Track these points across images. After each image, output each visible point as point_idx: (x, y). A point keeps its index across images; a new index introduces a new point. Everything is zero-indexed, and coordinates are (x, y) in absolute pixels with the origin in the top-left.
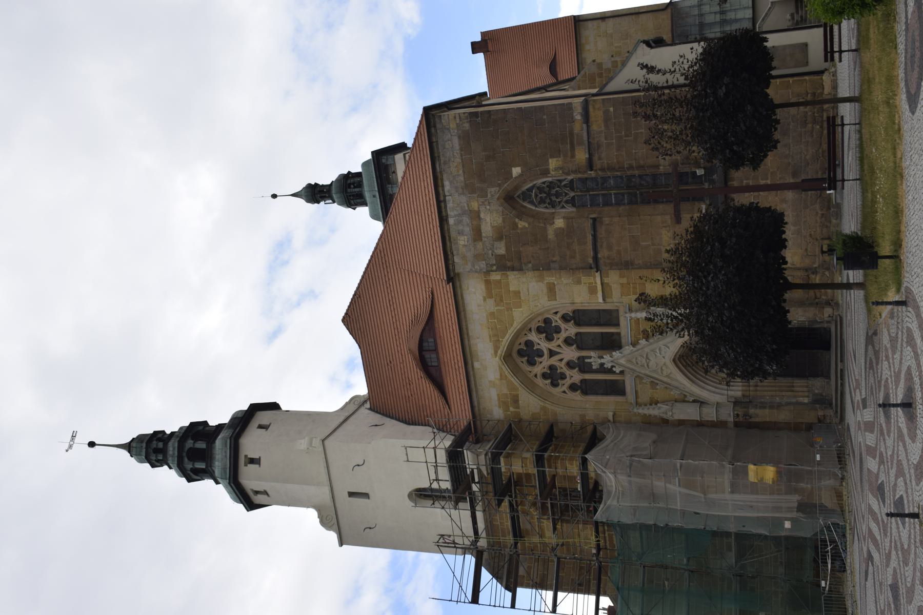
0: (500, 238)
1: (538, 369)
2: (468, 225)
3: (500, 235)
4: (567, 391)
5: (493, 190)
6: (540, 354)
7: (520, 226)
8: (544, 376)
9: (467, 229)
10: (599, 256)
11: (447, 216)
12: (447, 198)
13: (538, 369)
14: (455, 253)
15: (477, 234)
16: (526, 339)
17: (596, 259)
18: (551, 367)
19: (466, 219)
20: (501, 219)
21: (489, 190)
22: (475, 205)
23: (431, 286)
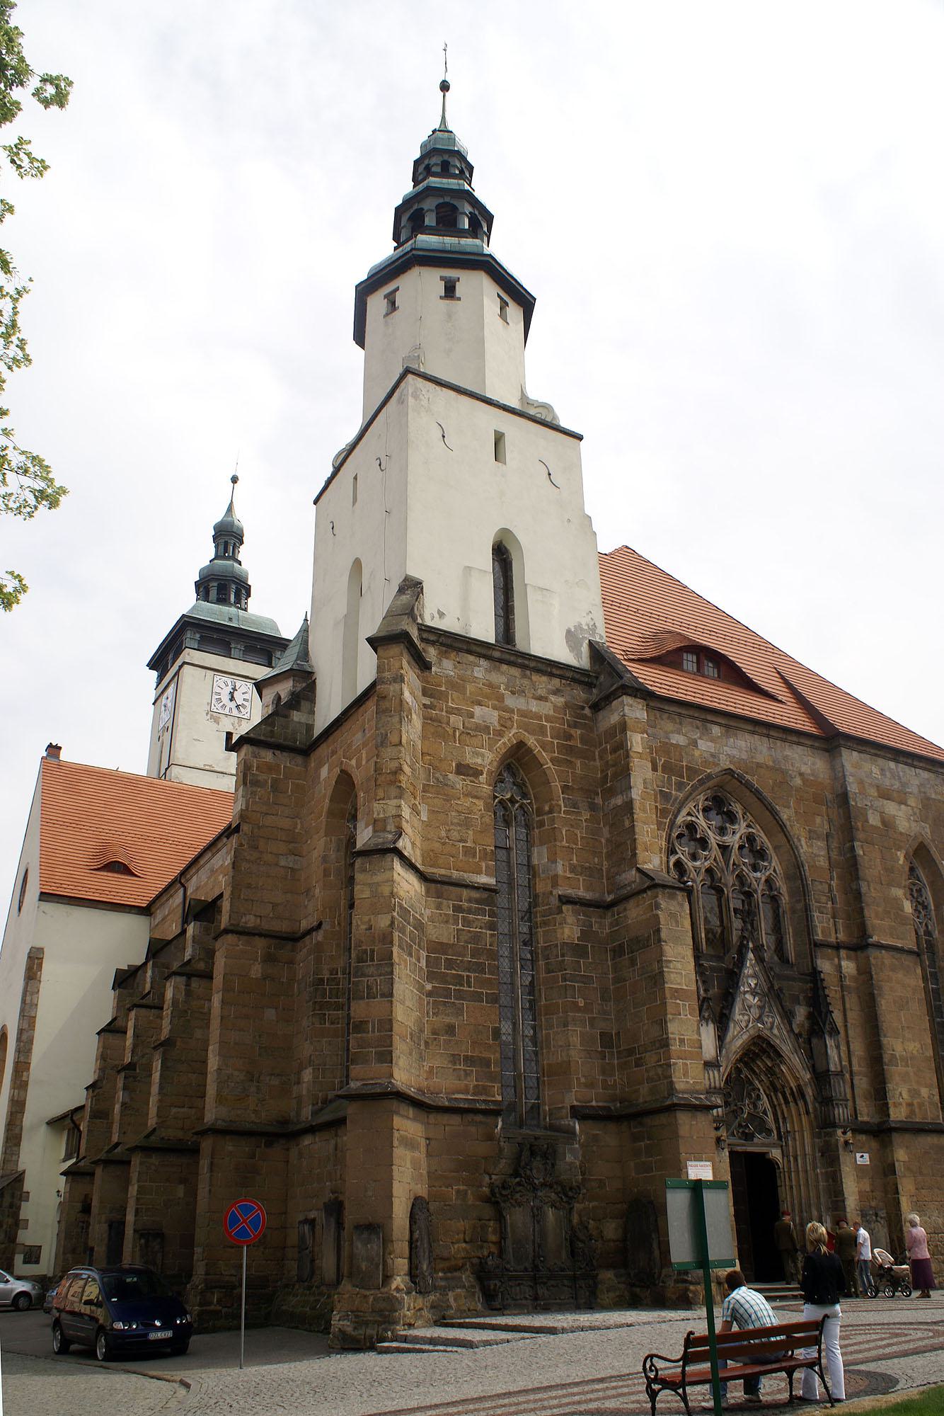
0: (884, 822)
1: (701, 821)
2: (892, 786)
3: (888, 823)
4: (677, 857)
5: (928, 830)
6: (722, 831)
7: (899, 853)
8: (691, 827)
9: (887, 782)
10: (883, 952)
11: (897, 762)
12: (913, 769)
13: (701, 821)
14: (862, 755)
15: (885, 795)
16: (740, 815)
17: (880, 946)
18: (703, 843)
19: (897, 785)
20: (903, 831)
21: (928, 826)
22: (911, 802)
23: (789, 704)
